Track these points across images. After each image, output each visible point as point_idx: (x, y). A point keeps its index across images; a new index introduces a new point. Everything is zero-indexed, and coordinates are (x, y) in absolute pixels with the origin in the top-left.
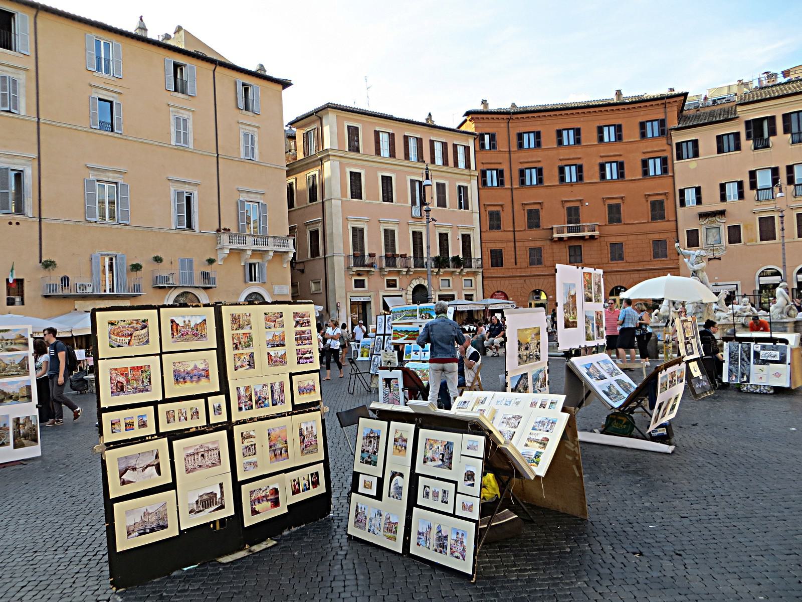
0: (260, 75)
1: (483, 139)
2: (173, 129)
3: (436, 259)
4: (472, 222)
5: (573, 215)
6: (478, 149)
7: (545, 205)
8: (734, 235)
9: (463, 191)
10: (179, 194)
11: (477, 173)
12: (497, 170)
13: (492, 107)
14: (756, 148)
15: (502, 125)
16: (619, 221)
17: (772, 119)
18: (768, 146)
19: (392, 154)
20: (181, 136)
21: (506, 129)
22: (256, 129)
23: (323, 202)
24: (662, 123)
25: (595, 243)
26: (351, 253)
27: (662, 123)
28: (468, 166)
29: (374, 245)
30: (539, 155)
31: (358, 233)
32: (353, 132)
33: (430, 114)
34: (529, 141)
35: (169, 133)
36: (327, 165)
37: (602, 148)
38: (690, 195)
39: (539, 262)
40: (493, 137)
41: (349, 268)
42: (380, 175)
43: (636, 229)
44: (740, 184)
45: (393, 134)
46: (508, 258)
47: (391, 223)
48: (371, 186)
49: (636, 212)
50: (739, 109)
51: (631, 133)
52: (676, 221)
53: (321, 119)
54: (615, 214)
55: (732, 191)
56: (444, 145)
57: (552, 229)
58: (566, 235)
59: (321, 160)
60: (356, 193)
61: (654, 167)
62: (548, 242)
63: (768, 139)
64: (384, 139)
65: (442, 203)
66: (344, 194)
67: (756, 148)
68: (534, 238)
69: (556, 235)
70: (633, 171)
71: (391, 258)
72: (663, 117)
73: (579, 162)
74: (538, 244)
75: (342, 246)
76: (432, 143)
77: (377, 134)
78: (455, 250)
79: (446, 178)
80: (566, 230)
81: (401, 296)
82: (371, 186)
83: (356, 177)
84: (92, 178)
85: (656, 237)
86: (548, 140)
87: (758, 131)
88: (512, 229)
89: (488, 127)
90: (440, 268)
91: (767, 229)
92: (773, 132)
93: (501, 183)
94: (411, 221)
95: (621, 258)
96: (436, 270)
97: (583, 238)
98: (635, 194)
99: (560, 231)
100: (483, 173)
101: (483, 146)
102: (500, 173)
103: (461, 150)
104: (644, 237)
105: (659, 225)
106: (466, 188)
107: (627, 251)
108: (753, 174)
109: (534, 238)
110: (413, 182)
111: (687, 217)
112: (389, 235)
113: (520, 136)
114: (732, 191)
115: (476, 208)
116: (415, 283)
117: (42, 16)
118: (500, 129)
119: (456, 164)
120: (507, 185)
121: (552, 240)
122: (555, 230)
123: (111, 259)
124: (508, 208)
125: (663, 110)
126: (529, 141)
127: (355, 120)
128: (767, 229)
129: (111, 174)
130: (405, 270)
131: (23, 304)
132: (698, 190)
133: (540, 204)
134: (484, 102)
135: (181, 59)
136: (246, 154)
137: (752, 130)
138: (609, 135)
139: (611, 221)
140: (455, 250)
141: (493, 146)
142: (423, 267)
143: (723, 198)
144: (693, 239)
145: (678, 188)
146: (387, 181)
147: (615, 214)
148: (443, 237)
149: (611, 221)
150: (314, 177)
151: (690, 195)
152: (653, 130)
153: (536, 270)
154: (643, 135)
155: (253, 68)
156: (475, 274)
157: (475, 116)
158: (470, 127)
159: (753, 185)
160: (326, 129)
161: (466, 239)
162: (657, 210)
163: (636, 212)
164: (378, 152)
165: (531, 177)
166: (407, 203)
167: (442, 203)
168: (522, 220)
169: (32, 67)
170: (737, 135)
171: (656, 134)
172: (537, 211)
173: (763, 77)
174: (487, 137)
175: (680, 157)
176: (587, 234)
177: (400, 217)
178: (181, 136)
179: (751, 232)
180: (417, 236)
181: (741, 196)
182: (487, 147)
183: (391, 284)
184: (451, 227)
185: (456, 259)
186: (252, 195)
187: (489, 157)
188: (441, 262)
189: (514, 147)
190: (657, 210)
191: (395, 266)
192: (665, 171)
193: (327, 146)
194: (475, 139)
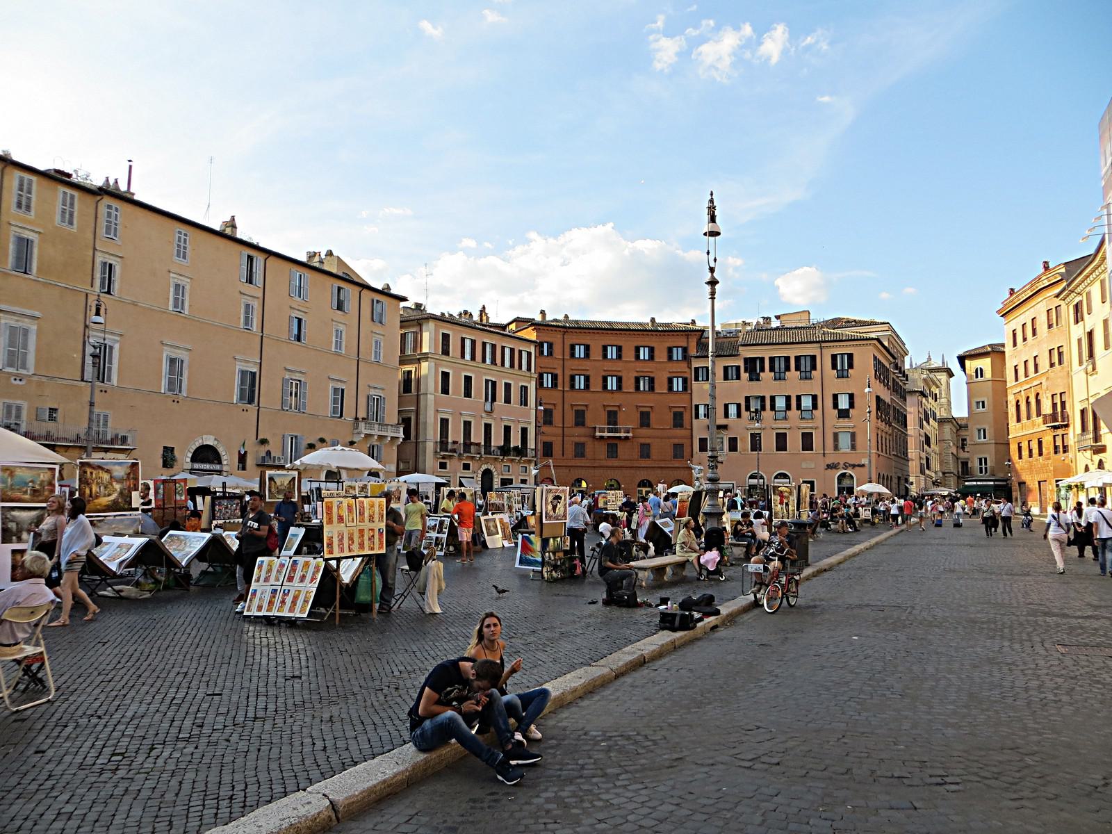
0: (385, 292)
1: (543, 347)
2: (334, 339)
3: (499, 448)
4: (530, 417)
5: (612, 417)
6: (538, 355)
7: (590, 407)
9: (524, 389)
10: (336, 390)
11: (536, 376)
12: (552, 374)
13: (549, 318)
14: (751, 379)
15: (559, 336)
16: (648, 425)
17: (762, 360)
18: (758, 379)
19: (473, 358)
20: (339, 345)
21: (561, 340)
22: (382, 337)
23: (418, 396)
24: (685, 350)
25: (628, 444)
26: (439, 440)
27: (685, 350)
28: (529, 369)
29: (456, 434)
30: (586, 365)
31: (444, 422)
32: (446, 337)
33: (484, 307)
34: (580, 352)
35: (332, 342)
36: (425, 365)
37: (637, 364)
39: (583, 455)
40: (550, 346)
41: (436, 452)
42: (463, 374)
43: (661, 436)
44: (739, 406)
45: (475, 341)
46: (557, 449)
47: (470, 415)
48: (456, 384)
49: (661, 419)
50: (740, 348)
51: (661, 356)
52: (692, 429)
53: (421, 325)
54: (645, 419)
55: (733, 410)
56: (512, 350)
57: (595, 428)
58: (606, 434)
59: (419, 359)
60: (445, 390)
61: (678, 385)
62: (591, 439)
63: (759, 374)
64: (468, 344)
65: (507, 400)
66: (436, 390)
67: (751, 379)
68: (578, 434)
69: (598, 434)
70: (661, 387)
71: (468, 445)
72: (686, 346)
73: (620, 374)
74: (582, 440)
75: (432, 433)
76: (503, 348)
77: (463, 340)
78: (515, 441)
79: (513, 379)
80: (606, 430)
81: (473, 478)
82: (456, 384)
83: (445, 376)
84: (287, 377)
85: (676, 441)
86: (596, 354)
87: (753, 367)
88: (561, 425)
89: (547, 337)
90: (504, 456)
91: (756, 444)
92: (762, 370)
93: (555, 385)
94: (484, 415)
95: (648, 456)
96: (501, 457)
97: (619, 438)
98: (661, 405)
99: (602, 430)
100: (541, 376)
101: (542, 352)
102: (555, 377)
103: (524, 355)
104: (667, 440)
105: (678, 432)
106: (526, 388)
107: (654, 452)
108: (747, 399)
109: (578, 434)
110: (487, 381)
111: (700, 427)
112: (467, 425)
113: (573, 347)
114: (733, 410)
115: (533, 405)
116: (484, 467)
117: (271, 260)
118: (556, 339)
119: (520, 367)
120: (560, 388)
121: (594, 437)
122: (597, 430)
123: (292, 439)
124: (560, 407)
125: (686, 340)
126: (580, 352)
127: (448, 329)
128: (756, 444)
129: (297, 374)
130: (478, 456)
131: (244, 469)
133: (586, 406)
134: (543, 312)
135: (342, 284)
136: (376, 357)
137: (748, 366)
138: (644, 354)
139: (642, 425)
140: (515, 441)
141: (550, 353)
142: (491, 454)
143: (726, 415)
145: (693, 404)
146: (468, 379)
147: (645, 419)
148: (507, 430)
149: (642, 425)
150: (410, 372)
151: (702, 410)
152: (677, 354)
153: (579, 462)
154: (670, 358)
155: (380, 287)
156: (529, 462)
157: (538, 327)
158: (531, 334)
159: (748, 408)
160: (426, 336)
161: (524, 431)
162: (678, 420)
163: (661, 419)
164: (463, 356)
165: (580, 383)
166: (481, 398)
167: (507, 400)
168: (570, 418)
169: (261, 295)
170: (738, 368)
171: (680, 358)
172: (583, 411)
173: (761, 321)
174: (545, 345)
175: (697, 379)
176: (623, 434)
177: (474, 410)
178: (339, 345)
179: (744, 444)
180: (488, 427)
181: (739, 415)
182: (545, 353)
183: (466, 467)
184: (513, 421)
185: (516, 448)
186: (377, 390)
187: (546, 362)
188: (505, 450)
189: (567, 356)
190: (678, 420)
191: (470, 452)
192: (685, 388)
193: (425, 350)
194: (536, 346)
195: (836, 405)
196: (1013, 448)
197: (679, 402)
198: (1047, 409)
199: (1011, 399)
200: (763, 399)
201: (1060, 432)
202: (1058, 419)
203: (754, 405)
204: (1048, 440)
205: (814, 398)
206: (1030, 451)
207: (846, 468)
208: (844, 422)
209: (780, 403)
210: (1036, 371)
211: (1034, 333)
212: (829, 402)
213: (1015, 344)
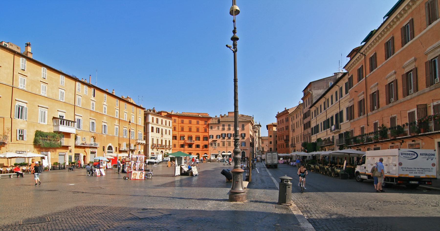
8: (219, 144)
9: (170, 131)
29: (155, 142)
38: (211, 136)
55: (218, 137)
65: (166, 134)
68: (182, 142)
111: (210, 140)
112: (158, 140)
114: (218, 137)
116: (161, 150)
148: (166, 141)
161: (169, 141)
167: (166, 134)
179: (221, 144)
180: (162, 140)
187: (175, 124)
197: (206, 134)
198: (285, 137)
200: (225, 134)
202: (287, 140)
203: (224, 136)
204: (285, 144)
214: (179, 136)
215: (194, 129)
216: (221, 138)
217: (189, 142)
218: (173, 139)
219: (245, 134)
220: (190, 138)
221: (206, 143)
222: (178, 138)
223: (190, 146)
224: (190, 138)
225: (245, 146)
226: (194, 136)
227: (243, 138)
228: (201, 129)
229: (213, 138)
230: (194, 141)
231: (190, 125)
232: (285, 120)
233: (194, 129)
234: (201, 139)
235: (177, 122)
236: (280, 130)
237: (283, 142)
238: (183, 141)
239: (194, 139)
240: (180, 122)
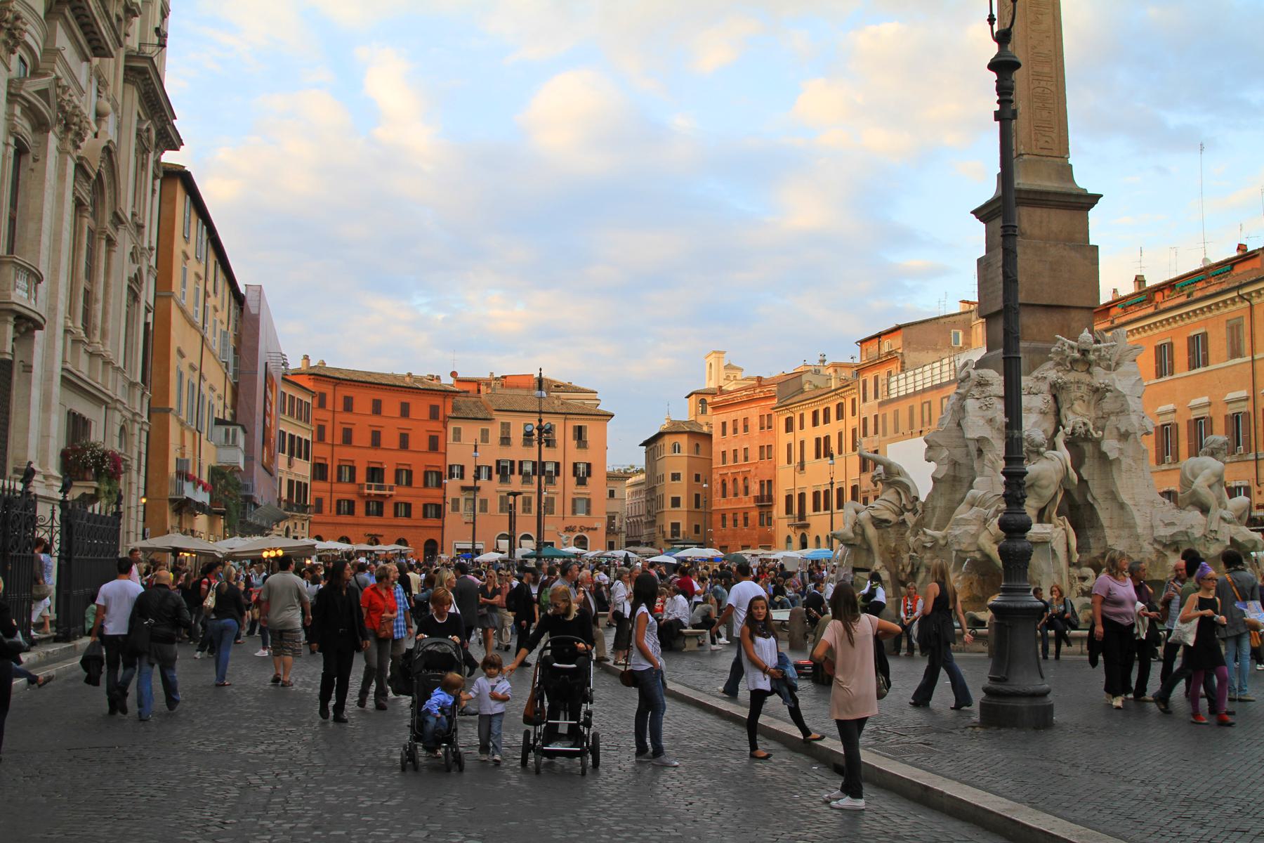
6: (316, 405)
55: (484, 472)
68: (346, 491)
69: (367, 491)
99: (370, 488)
108: (498, 462)
111: (452, 486)
118: (327, 389)
132: (462, 468)
134: (306, 358)
144: (456, 507)
176: (387, 492)
181: (490, 478)
195: (575, 474)
196: (717, 518)
197: (433, 460)
198: (755, 489)
199: (716, 476)
200: (512, 463)
201: (765, 510)
202: (765, 501)
204: (754, 514)
205: (557, 465)
206: (735, 520)
207: (581, 531)
208: (582, 489)
209: (528, 468)
210: (746, 459)
211: (746, 428)
212: (569, 470)
213: (724, 433)
214: (336, 464)
215: (390, 438)
216: (496, 477)
217: (373, 492)
218: (314, 478)
219: (589, 465)
220: (375, 474)
221: (433, 494)
222: (332, 473)
223: (376, 506)
224: (375, 474)
225: (588, 512)
226: (390, 460)
227: (581, 482)
228: (419, 441)
229: (462, 477)
230: (391, 488)
231: (375, 420)
232: (754, 422)
233: (390, 438)
234: (418, 479)
235: (329, 406)
236: (730, 456)
237: (748, 502)
238: (351, 487)
239: (389, 479)
240: (340, 407)
